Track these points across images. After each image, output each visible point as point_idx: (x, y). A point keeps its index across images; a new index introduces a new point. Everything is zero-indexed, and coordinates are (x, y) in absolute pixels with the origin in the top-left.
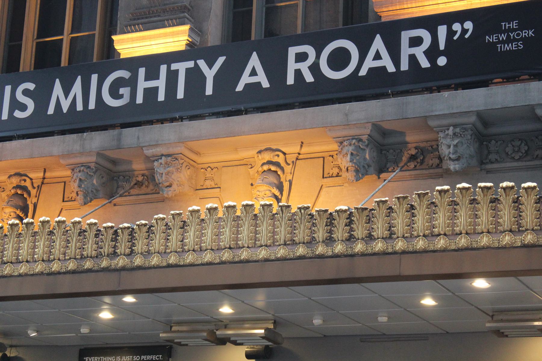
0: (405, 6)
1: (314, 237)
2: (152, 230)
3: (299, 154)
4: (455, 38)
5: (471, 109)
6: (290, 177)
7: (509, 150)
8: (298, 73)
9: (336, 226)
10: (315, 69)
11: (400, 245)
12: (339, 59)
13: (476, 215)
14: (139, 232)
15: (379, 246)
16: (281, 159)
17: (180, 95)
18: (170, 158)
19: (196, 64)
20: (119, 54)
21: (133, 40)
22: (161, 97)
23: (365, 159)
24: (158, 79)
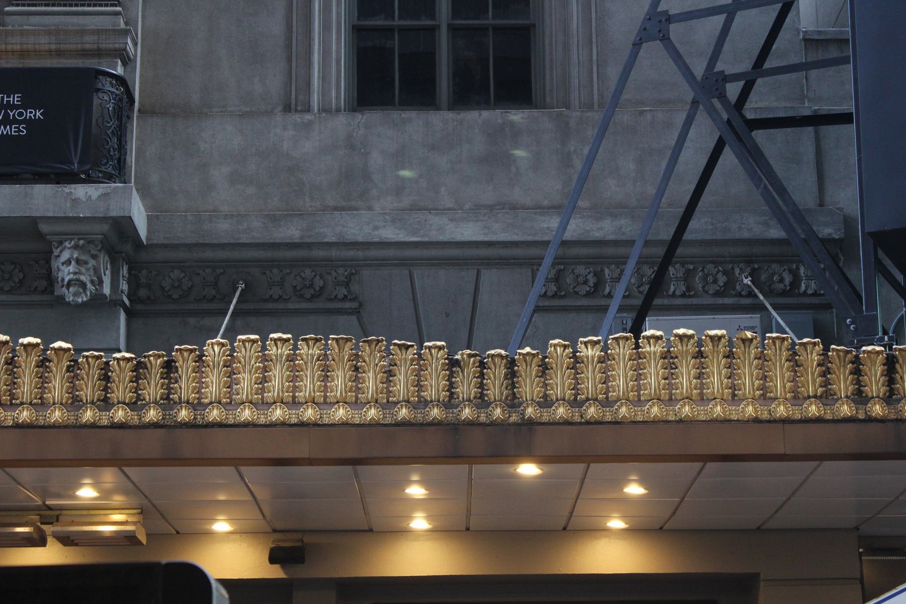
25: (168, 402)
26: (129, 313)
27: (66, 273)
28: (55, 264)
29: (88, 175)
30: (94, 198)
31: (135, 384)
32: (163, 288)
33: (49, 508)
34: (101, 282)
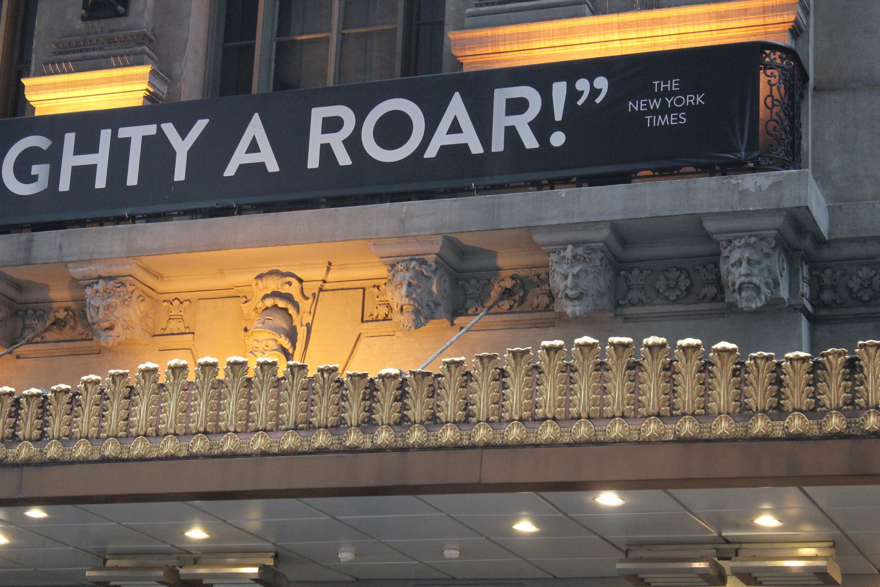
0: (502, 49)
1: (343, 418)
2: (77, 401)
3: (324, 282)
4: (580, 102)
5: (603, 218)
6: (308, 319)
7: (661, 284)
8: (326, 151)
9: (379, 402)
10: (353, 144)
11: (482, 434)
12: (393, 130)
13: (605, 388)
14: (55, 403)
15: (448, 435)
16: (294, 290)
17: (132, 179)
18: (112, 282)
19: (159, 130)
20: (33, 109)
21: (56, 87)
22: (101, 182)
23: (430, 293)
24: (96, 151)
25: (852, 407)
26: (813, 321)
27: (735, 274)
28: (723, 267)
29: (757, 163)
30: (764, 188)
31: (813, 388)
32: (850, 290)
33: (727, 541)
34: (777, 284)
